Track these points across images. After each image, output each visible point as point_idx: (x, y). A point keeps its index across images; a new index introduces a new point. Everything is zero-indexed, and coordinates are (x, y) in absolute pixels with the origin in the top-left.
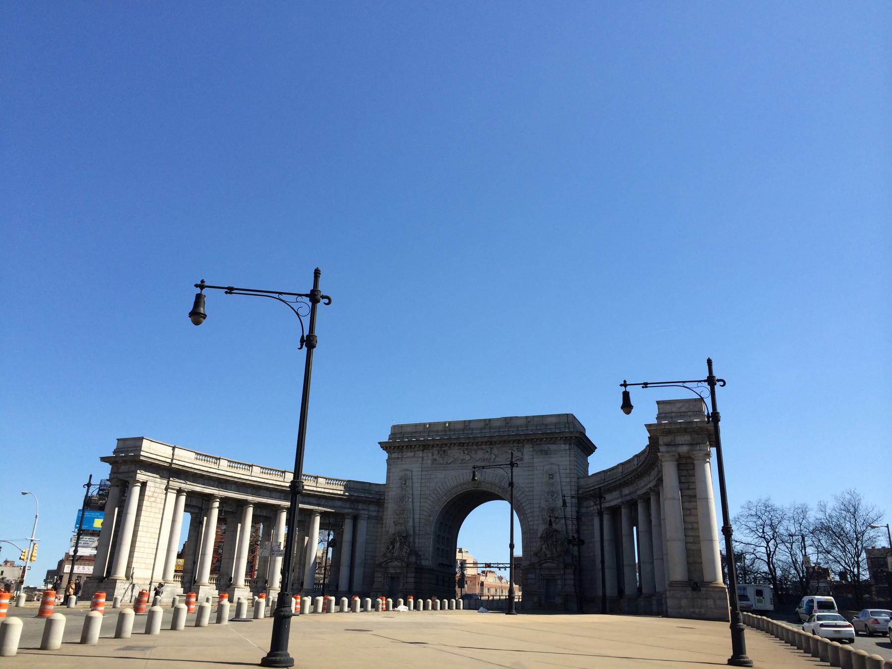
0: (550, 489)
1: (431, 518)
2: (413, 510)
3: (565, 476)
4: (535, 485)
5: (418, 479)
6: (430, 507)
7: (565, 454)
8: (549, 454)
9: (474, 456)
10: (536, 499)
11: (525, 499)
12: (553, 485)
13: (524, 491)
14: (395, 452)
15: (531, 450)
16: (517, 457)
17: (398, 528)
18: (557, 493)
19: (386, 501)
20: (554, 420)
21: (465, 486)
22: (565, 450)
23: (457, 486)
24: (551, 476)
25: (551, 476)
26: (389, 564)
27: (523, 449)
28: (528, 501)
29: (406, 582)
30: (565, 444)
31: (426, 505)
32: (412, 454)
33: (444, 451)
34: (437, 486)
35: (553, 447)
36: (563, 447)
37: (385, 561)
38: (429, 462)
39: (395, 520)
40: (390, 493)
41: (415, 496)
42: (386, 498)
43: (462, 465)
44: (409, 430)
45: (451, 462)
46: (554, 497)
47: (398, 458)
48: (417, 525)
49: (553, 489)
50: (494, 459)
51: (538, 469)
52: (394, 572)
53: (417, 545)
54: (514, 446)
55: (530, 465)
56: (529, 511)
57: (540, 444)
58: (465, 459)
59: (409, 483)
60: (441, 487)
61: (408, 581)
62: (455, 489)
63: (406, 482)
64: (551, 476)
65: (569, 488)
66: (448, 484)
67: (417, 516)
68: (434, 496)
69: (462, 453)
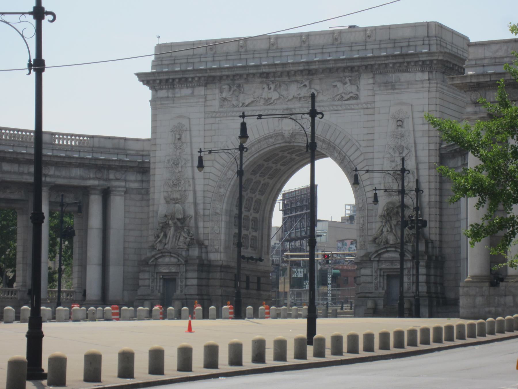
5: (199, 130)
6: (219, 174)
7: (423, 87)
9: (284, 93)
14: (162, 89)
15: (371, 81)
16: (352, 92)
26: (160, 260)
30: (423, 71)
48: (200, 200)
52: (167, 271)
58: (271, 98)
59: (186, 137)
61: (188, 283)
63: (180, 135)
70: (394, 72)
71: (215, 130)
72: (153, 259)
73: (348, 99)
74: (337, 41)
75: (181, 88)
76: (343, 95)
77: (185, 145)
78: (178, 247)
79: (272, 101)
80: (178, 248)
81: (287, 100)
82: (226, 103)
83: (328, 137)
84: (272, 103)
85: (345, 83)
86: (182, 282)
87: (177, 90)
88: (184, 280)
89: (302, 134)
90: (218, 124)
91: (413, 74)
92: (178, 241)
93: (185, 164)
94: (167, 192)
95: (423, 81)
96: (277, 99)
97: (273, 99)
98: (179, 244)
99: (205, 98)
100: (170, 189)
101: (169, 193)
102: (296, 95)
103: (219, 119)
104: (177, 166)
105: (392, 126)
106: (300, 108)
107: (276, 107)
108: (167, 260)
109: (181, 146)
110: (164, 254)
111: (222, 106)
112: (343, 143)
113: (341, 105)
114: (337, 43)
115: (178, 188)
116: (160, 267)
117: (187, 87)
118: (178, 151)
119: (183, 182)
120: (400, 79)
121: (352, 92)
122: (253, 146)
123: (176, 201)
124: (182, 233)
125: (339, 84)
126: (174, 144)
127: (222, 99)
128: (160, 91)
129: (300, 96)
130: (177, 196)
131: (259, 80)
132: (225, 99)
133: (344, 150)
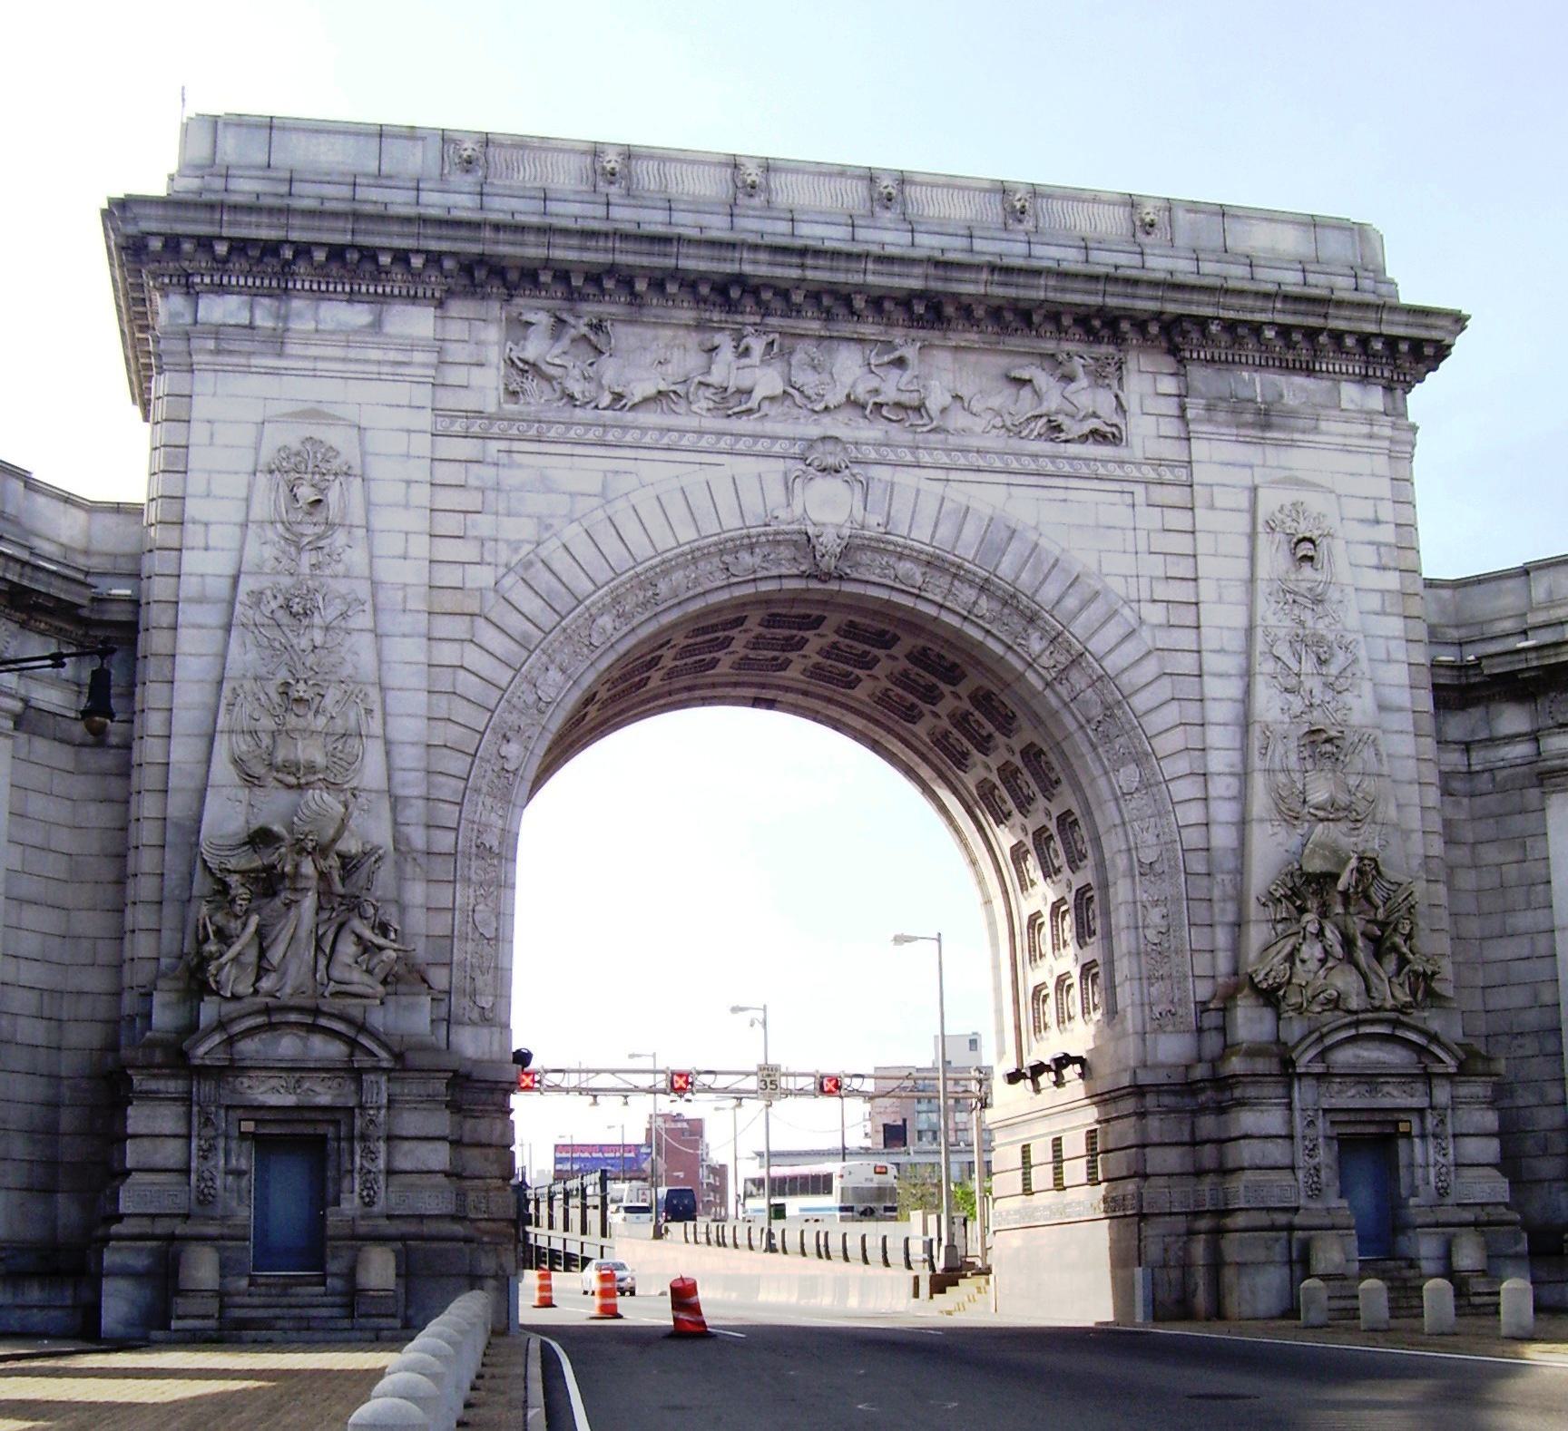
0: (1302, 623)
1: (513, 750)
2: (383, 689)
3: (1374, 561)
4: (1207, 590)
5: (408, 482)
6: (504, 676)
7: (1371, 437)
8: (1281, 428)
9: (800, 378)
11: (1150, 668)
12: (1318, 601)
13: (1141, 621)
14: (221, 289)
15: (1169, 385)
16: (1095, 415)
17: (273, 808)
19: (156, 615)
21: (745, 557)
22: (1369, 416)
23: (695, 556)
24: (1305, 549)
25: (1305, 550)
26: (248, 1047)
27: (1120, 379)
28: (1166, 681)
29: (390, 1172)
30: (1364, 379)
31: (473, 658)
32: (359, 315)
33: (598, 327)
34: (553, 544)
35: (1295, 389)
36: (1350, 393)
37: (221, 1025)
39: (243, 745)
40: (193, 562)
41: (388, 597)
42: (159, 589)
44: (331, 155)
45: (646, 400)
46: (1333, 669)
47: (251, 327)
48: (412, 786)
49: (1321, 627)
50: (944, 410)
51: (1218, 504)
52: (290, 1100)
53: (417, 922)
56: (1174, 741)
58: (750, 392)
59: (343, 498)
60: (583, 550)
61: (402, 1163)
62: (678, 576)
63: (322, 491)
64: (1305, 549)
65: (1395, 625)
66: (632, 532)
67: (408, 728)
68: (532, 605)
69: (727, 353)
70: (1260, 367)
71: (482, 490)
72: (217, 1038)
73: (1083, 439)
74: (1020, 221)
75: (320, 296)
76: (1060, 418)
77: (340, 538)
78: (332, 987)
79: (753, 404)
80: (335, 994)
81: (819, 407)
82: (532, 385)
83: (1006, 568)
84: (749, 411)
85: (1069, 378)
86: (370, 1154)
87: (297, 304)
88: (382, 1146)
89: (891, 547)
90: (496, 464)
91: (1329, 383)
92: (330, 960)
93: (344, 616)
94: (253, 733)
95: (1369, 412)
96: (772, 399)
97: (758, 394)
98: (337, 973)
100: (267, 723)
101: (266, 741)
102: (861, 393)
103: (503, 445)
104: (306, 622)
105: (1273, 559)
106: (877, 445)
107: (769, 427)
108: (288, 1046)
109: (320, 537)
110: (276, 1018)
111: (515, 393)
112: (1071, 603)
113: (1053, 458)
114: (1021, 227)
115: (310, 715)
116: (246, 1082)
117: (352, 298)
118: (307, 559)
119: (333, 694)
120: (1281, 396)
121: (1095, 415)
122: (665, 573)
123: (297, 777)
124: (357, 924)
125: (1042, 379)
126: (288, 526)
127: (521, 365)
128: (211, 296)
129: (879, 399)
130: (310, 751)
131: (687, 315)
132: (530, 368)
133: (1078, 627)
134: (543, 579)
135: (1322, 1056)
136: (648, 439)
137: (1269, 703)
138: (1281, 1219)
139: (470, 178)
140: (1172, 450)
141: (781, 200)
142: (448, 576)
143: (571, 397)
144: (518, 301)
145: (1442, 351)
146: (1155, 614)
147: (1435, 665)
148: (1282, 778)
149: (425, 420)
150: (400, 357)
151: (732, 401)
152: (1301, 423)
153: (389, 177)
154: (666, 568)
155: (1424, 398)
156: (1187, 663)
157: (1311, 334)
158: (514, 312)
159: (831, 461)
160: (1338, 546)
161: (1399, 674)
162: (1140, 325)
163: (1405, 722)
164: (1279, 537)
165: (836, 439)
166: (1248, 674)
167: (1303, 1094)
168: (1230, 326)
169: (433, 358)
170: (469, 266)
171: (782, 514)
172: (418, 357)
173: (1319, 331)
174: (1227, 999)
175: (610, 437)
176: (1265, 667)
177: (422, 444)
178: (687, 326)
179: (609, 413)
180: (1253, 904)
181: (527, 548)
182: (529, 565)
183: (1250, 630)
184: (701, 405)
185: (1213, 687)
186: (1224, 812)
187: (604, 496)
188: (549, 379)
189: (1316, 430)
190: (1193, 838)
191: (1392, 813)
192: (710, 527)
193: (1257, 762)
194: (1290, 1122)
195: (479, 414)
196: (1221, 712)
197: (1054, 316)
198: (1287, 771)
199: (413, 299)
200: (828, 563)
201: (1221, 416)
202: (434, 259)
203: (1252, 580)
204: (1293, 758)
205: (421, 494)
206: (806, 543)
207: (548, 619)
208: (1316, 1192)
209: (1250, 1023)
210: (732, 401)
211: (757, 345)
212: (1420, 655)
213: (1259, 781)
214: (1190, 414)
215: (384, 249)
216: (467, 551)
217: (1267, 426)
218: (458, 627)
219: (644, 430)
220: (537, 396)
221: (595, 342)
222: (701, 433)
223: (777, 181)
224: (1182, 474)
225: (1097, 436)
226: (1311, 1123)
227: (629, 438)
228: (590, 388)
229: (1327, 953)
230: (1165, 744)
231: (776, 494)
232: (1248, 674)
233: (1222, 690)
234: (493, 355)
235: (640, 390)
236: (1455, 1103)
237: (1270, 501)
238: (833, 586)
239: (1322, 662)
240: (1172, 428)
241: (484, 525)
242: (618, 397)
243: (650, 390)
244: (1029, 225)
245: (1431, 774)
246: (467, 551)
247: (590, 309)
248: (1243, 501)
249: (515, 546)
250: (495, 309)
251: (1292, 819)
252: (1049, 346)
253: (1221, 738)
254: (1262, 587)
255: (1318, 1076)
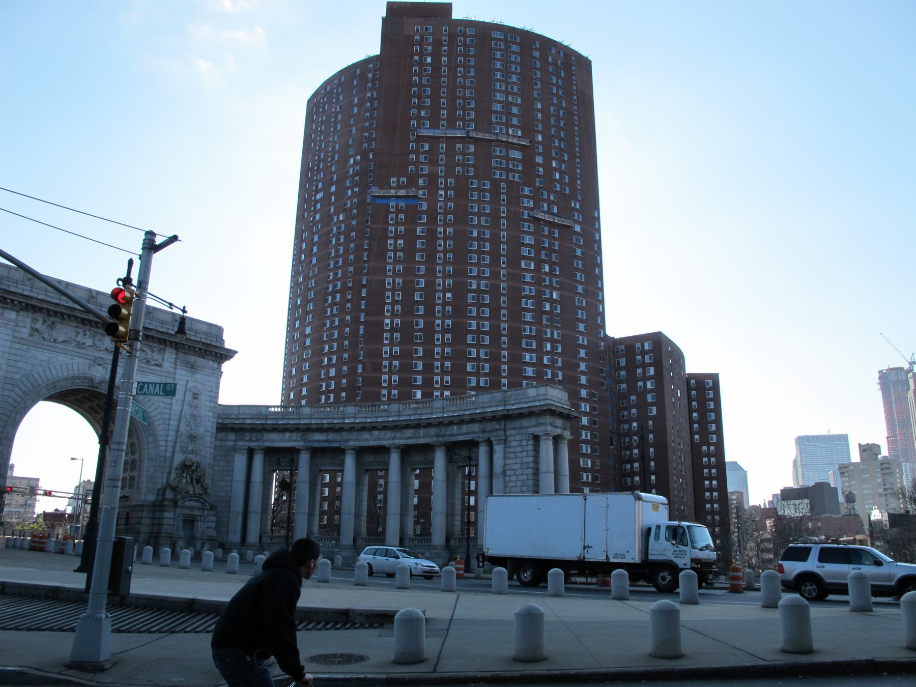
5: (4, 352)
6: (19, 400)
7: (213, 373)
9: (96, 342)
10: (174, 420)
11: (159, 416)
13: (159, 406)
15: (174, 356)
16: (157, 360)
18: (200, 418)
20: (205, 328)
21: (77, 380)
23: (66, 379)
24: (196, 396)
27: (164, 353)
30: (214, 361)
33: (53, 323)
34: (35, 371)
35: (200, 361)
36: (211, 363)
38: (25, 332)
43: (78, 350)
45: (61, 342)
46: (197, 422)
54: (155, 347)
55: (170, 375)
57: (187, 354)
62: (62, 383)
64: (196, 396)
65: (211, 414)
66: (53, 370)
68: (28, 385)
69: (81, 335)
70: (193, 355)
73: (154, 365)
76: (150, 360)
82: (36, 334)
85: (153, 351)
90: (25, 351)
96: (89, 346)
97: (87, 344)
99: (16, 323)
103: (27, 347)
105: (189, 396)
107: (88, 353)
121: (157, 360)
125: (148, 351)
131: (74, 324)
132: (37, 330)
134: (31, 378)
135: (183, 503)
136: (60, 351)
137: (183, 428)
138: (171, 535)
139: (29, 282)
140: (172, 370)
141: (99, 301)
142: (10, 375)
143: (44, 338)
144: (36, 314)
145: (232, 357)
146: (162, 405)
147: (218, 423)
148: (183, 444)
149: (10, 338)
150: (7, 323)
151: (80, 345)
152: (200, 369)
153: (11, 279)
154: (59, 381)
155: (226, 366)
156: (167, 416)
157: (205, 350)
158: (35, 317)
159: (100, 363)
160: (203, 397)
161: (210, 424)
162: (171, 342)
163: (209, 434)
164: (191, 393)
165: (102, 358)
166: (180, 421)
167: (178, 510)
168: (189, 346)
169: (14, 324)
170: (27, 305)
171: (88, 372)
172: (11, 323)
173: (208, 350)
174: (165, 489)
175: (52, 349)
176: (183, 420)
177: (8, 344)
178: (73, 326)
179: (52, 344)
180: (173, 470)
181: (28, 371)
182: (28, 375)
183: (182, 411)
184: (73, 345)
185: (172, 422)
186: (170, 449)
187: (48, 362)
188: (40, 333)
189: (202, 371)
190: (163, 454)
191: (204, 453)
192: (71, 373)
193: (179, 440)
194: (175, 516)
195: (23, 339)
196: (173, 428)
197: (153, 337)
198: (184, 442)
199: (12, 310)
200: (95, 385)
201: (184, 365)
202: (20, 303)
203: (184, 400)
204: (186, 441)
205: (6, 355)
206: (91, 380)
207: (31, 388)
208: (177, 531)
209: (169, 495)
210: (80, 345)
211: (88, 334)
212: (215, 421)
213: (178, 444)
214: (178, 363)
215: (9, 298)
216: (14, 370)
217: (193, 368)
218: (9, 387)
219: (60, 349)
220: (37, 337)
221: (52, 327)
222: (72, 351)
223: (99, 296)
224: (173, 376)
225: (157, 365)
226: (179, 516)
227: (57, 350)
228: (49, 337)
229: (187, 482)
230: (160, 433)
231: (87, 368)
232: (180, 421)
233: (174, 423)
234: (28, 325)
235: (60, 340)
236: (208, 515)
237: (190, 384)
238: (95, 389)
239: (195, 420)
240: (173, 365)
241: (20, 364)
242: (55, 340)
243: (63, 340)
244: (151, 316)
245: (213, 446)
246: (14, 370)
247: (52, 319)
248: (185, 383)
249: (26, 370)
250: (30, 315)
251: (183, 452)
252: (151, 344)
253: (172, 434)
254: (185, 402)
255: (182, 507)
